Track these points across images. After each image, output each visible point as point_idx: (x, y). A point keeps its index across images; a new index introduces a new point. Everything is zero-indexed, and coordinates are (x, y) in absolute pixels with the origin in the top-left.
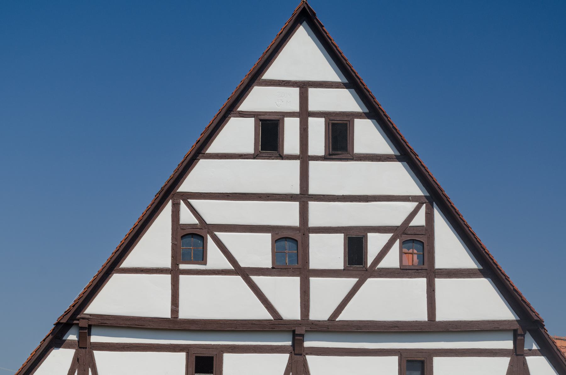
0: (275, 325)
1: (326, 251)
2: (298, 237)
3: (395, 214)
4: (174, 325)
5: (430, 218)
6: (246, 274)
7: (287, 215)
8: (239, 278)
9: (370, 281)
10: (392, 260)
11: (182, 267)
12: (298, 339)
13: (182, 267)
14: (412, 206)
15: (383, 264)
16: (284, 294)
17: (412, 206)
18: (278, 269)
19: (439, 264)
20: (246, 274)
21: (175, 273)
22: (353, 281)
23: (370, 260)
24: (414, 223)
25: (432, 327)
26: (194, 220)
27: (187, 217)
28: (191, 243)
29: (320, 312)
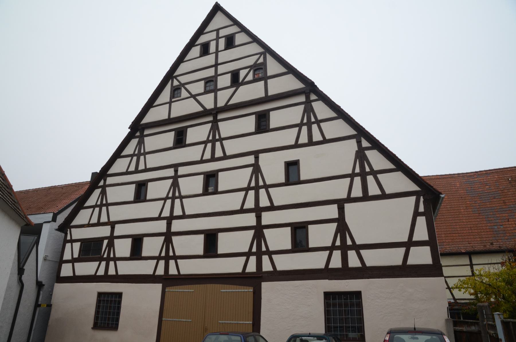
0: (205, 113)
1: (224, 81)
2: (214, 79)
3: (251, 61)
4: (170, 121)
5: (265, 59)
6: (194, 97)
7: (211, 72)
8: (192, 99)
9: (241, 87)
10: (250, 77)
11: (173, 100)
12: (215, 117)
13: (173, 100)
14: (258, 56)
15: (246, 80)
16: (208, 101)
17: (258, 56)
18: (206, 92)
19: (269, 74)
20: (194, 97)
21: (170, 103)
22: (234, 89)
23: (241, 80)
24: (259, 62)
25: (267, 99)
26: (178, 84)
27: (176, 83)
28: (175, 91)
29: (221, 103)
